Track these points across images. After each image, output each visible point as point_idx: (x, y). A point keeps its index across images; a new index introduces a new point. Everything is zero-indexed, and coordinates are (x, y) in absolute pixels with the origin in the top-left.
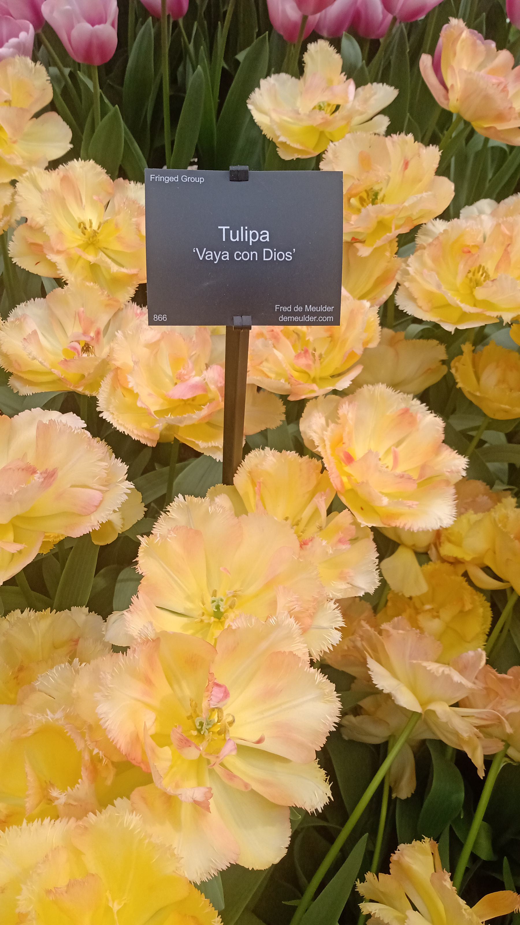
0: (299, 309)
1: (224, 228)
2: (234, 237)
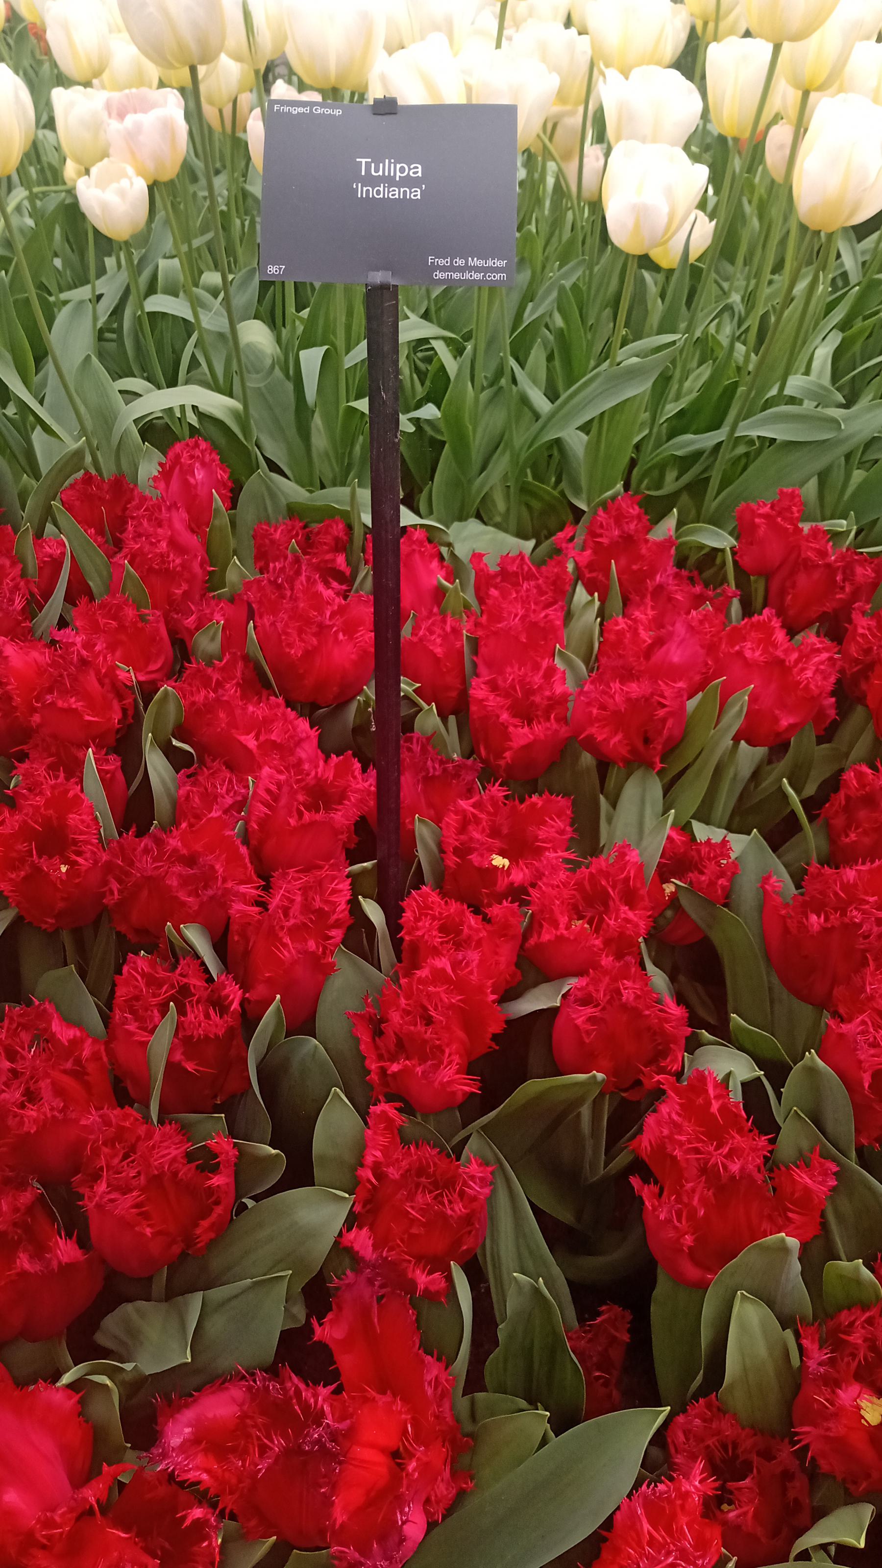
0: (460, 262)
1: (364, 161)
2: (377, 171)
